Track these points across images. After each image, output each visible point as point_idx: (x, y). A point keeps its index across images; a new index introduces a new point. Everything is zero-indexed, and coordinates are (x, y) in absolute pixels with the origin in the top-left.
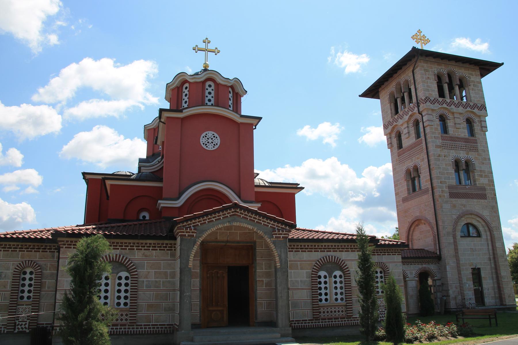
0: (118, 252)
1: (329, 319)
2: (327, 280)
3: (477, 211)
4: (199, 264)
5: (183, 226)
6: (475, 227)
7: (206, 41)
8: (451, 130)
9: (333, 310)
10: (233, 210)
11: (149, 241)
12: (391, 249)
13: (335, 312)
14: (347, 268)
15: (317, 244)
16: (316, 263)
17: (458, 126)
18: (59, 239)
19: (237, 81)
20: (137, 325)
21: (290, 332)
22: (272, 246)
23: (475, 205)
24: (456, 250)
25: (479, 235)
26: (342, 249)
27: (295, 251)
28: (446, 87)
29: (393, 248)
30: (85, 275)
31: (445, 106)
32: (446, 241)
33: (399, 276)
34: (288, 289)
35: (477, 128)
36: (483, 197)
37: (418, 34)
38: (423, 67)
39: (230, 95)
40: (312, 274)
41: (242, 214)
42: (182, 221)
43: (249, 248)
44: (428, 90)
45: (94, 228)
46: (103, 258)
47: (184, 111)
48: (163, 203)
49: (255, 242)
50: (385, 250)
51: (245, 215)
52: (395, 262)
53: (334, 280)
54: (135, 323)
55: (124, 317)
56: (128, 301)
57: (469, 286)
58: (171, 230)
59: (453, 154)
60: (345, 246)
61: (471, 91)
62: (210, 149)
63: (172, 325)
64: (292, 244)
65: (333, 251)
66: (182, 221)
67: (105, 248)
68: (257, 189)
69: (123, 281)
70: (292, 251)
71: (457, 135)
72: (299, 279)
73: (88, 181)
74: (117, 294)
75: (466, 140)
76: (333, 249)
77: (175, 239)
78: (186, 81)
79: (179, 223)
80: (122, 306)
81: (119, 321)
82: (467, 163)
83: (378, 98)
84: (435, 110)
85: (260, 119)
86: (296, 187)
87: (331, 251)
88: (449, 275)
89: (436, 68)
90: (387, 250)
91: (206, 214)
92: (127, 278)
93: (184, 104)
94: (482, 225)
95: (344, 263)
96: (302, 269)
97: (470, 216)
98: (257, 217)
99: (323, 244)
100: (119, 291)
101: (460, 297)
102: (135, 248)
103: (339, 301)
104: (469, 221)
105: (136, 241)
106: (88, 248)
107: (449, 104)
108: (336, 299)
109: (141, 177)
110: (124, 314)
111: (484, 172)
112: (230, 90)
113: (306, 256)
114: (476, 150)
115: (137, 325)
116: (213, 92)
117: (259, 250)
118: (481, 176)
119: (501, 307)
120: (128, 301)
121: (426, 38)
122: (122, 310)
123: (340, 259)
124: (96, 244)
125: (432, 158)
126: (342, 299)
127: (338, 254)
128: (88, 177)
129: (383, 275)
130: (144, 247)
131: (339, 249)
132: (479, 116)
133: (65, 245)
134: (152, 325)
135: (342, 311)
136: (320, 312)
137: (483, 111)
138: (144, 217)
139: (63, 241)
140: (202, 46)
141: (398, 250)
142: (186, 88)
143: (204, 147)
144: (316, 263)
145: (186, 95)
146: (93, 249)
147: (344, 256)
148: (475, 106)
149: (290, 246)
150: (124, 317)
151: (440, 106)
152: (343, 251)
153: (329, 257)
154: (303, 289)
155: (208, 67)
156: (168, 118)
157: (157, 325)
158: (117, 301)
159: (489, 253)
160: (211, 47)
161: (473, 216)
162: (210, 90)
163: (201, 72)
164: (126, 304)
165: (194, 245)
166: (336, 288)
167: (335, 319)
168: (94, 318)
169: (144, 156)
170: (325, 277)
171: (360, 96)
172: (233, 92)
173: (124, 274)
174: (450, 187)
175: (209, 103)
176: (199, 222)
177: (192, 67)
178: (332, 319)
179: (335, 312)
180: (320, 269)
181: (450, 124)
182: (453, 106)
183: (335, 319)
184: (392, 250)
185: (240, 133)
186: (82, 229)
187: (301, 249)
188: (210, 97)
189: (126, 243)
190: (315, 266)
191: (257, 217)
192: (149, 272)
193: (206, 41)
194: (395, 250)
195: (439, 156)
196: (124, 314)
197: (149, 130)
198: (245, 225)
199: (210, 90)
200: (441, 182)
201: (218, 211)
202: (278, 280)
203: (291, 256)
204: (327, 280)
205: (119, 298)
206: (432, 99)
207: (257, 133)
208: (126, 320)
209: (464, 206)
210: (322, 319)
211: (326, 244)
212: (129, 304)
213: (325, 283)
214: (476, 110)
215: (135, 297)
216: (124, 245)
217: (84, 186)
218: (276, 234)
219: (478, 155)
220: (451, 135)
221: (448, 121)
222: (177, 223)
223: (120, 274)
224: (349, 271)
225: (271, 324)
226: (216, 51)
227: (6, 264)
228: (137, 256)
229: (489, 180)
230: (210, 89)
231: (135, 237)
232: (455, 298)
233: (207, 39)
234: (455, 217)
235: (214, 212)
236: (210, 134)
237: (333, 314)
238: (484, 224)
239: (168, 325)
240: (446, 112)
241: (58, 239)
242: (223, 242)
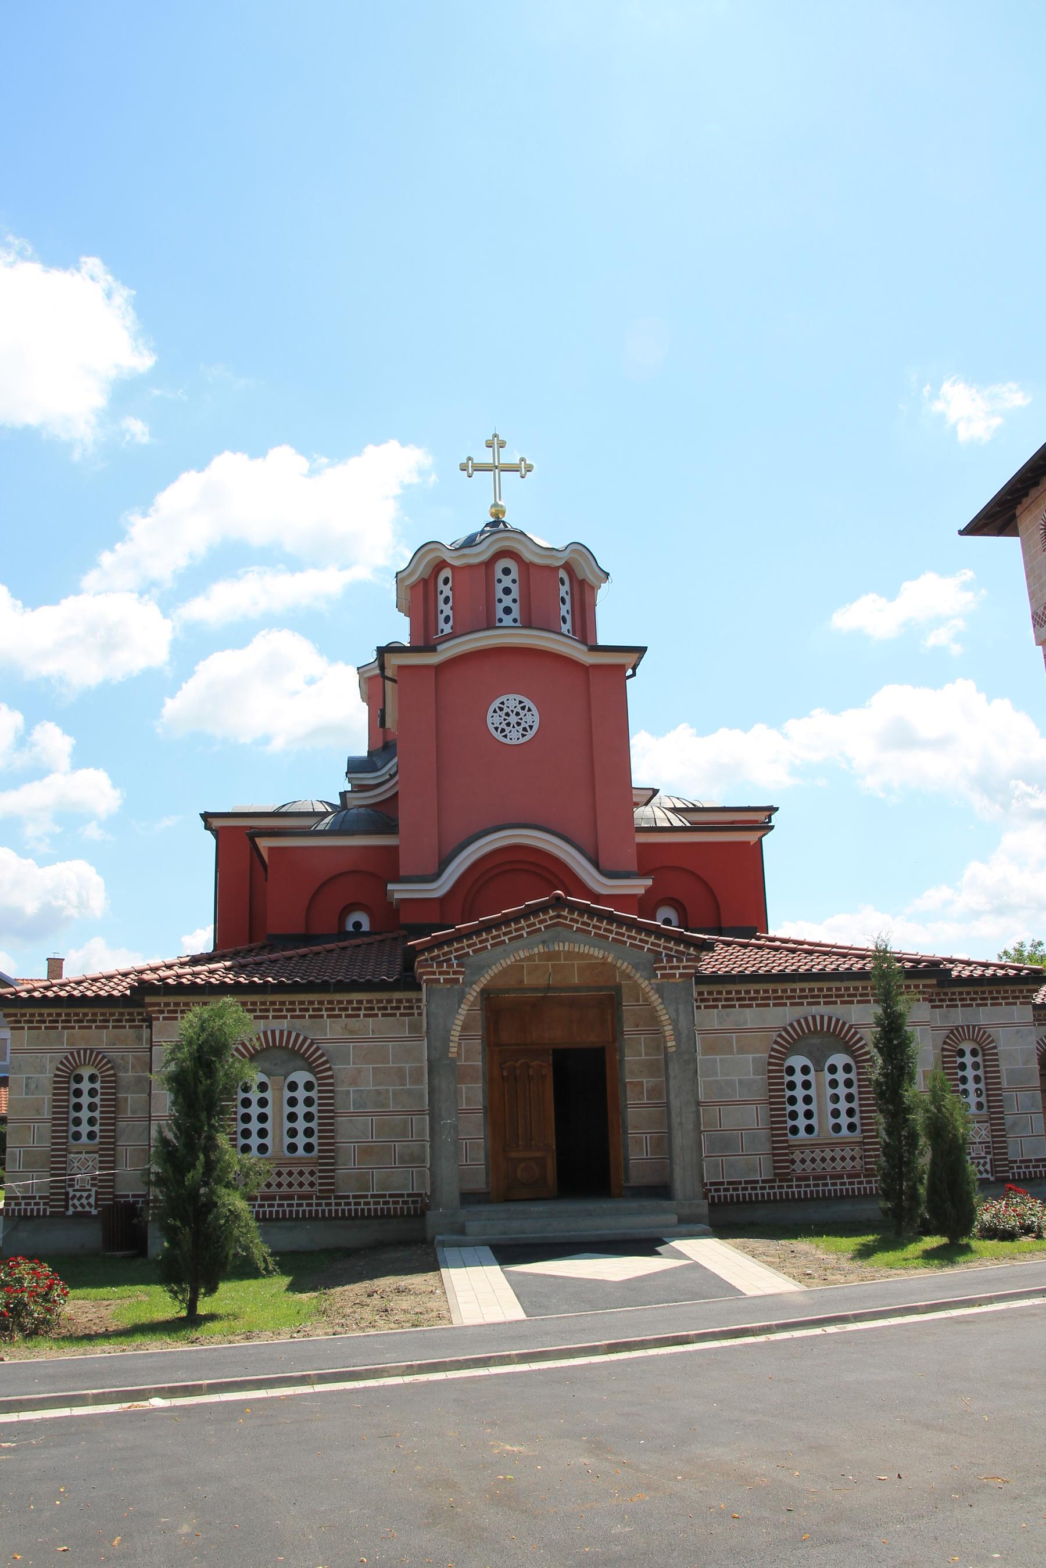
0: (285, 1024)
1: (815, 1178)
2: (811, 1077)
4: (480, 1048)
5: (432, 959)
7: (496, 443)
9: (828, 1154)
10: (552, 913)
11: (355, 996)
12: (1001, 988)
13: (843, 1159)
15: (779, 987)
16: (780, 1036)
18: (148, 1000)
19: (580, 549)
20: (336, 1197)
21: (705, 1210)
22: (654, 997)
26: (849, 996)
27: (723, 1006)
29: (1007, 987)
30: (200, 1087)
33: (1026, 1063)
34: (698, 1104)
39: (564, 590)
40: (770, 1064)
41: (577, 922)
42: (429, 948)
43: (607, 1001)
45: (226, 968)
46: (237, 1050)
47: (439, 648)
48: (399, 891)
49: (618, 988)
50: (983, 992)
51: (583, 923)
52: (1013, 1025)
53: (829, 1077)
54: (332, 1191)
55: (306, 1179)
56: (314, 1140)
58: (408, 967)
60: (856, 988)
62: (515, 742)
63: (420, 1195)
64: (705, 988)
65: (825, 1003)
66: (429, 948)
67: (240, 1023)
68: (641, 838)
69: (301, 1094)
70: (717, 1007)
73: (217, 833)
74: (288, 1125)
76: (825, 996)
77: (420, 989)
78: (442, 564)
79: (421, 952)
80: (301, 1151)
81: (296, 1188)
85: (642, 650)
86: (759, 820)
87: (819, 1003)
90: (991, 992)
91: (487, 927)
92: (309, 1086)
93: (442, 625)
95: (856, 1033)
96: (742, 1050)
98: (614, 927)
99: (798, 986)
100: (292, 1117)
102: (325, 1013)
103: (845, 1130)
105: (326, 997)
106: (203, 1029)
108: (837, 1128)
109: (345, 817)
110: (306, 1170)
112: (562, 574)
113: (751, 1017)
115: (336, 1197)
116: (515, 588)
117: (628, 1006)
120: (314, 1140)
122: (300, 1162)
123: (844, 1024)
124: (219, 1022)
126: (851, 1127)
127: (838, 1010)
128: (217, 823)
129: (979, 1059)
130: (346, 1009)
131: (842, 996)
133: (162, 1012)
134: (373, 1196)
135: (853, 1158)
136: (793, 1162)
138: (357, 925)
139: (159, 1005)
140: (485, 457)
141: (1021, 991)
142: (446, 581)
143: (498, 736)
144: (780, 1036)
145: (446, 600)
146: (212, 1035)
149: (700, 993)
150: (306, 1179)
152: (852, 1002)
153: (814, 1018)
154: (745, 1103)
155: (504, 513)
156: (400, 667)
157: (384, 1196)
158: (288, 1140)
160: (508, 457)
162: (507, 581)
163: (482, 532)
164: (309, 1148)
165: (460, 1003)
166: (835, 1099)
167: (832, 1177)
168: (219, 1181)
169: (362, 751)
170: (805, 1070)
171: (961, 533)
172: (566, 584)
173: (301, 1077)
175: (508, 620)
176: (469, 946)
177: (456, 523)
178: (824, 1178)
179: (833, 1159)
180: (793, 1048)
183: (832, 1177)
184: (1006, 992)
185: (595, 689)
186: (199, 973)
187: (739, 999)
188: (507, 601)
189: (302, 1003)
190: (776, 1042)
191: (614, 927)
192: (359, 1071)
193: (496, 443)
194: (1013, 991)
196: (306, 1170)
197: (370, 678)
198: (585, 949)
199: (507, 581)
201: (516, 918)
202: (672, 1082)
203: (710, 1019)
204: (811, 1077)
205: (293, 1133)
207: (638, 690)
208: (312, 1184)
210: (799, 1179)
211: (806, 985)
212: (316, 1148)
213: (806, 1085)
215: (328, 1131)
216: (297, 1007)
217: (209, 841)
218: (664, 968)
222: (415, 952)
223: (292, 1078)
225: (662, 1191)
226: (521, 468)
228: (329, 1031)
230: (507, 581)
231: (324, 987)
233: (495, 436)
235: (506, 920)
236: (512, 701)
237: (839, 1165)
239: (409, 1195)
241: (144, 998)
242: (536, 989)
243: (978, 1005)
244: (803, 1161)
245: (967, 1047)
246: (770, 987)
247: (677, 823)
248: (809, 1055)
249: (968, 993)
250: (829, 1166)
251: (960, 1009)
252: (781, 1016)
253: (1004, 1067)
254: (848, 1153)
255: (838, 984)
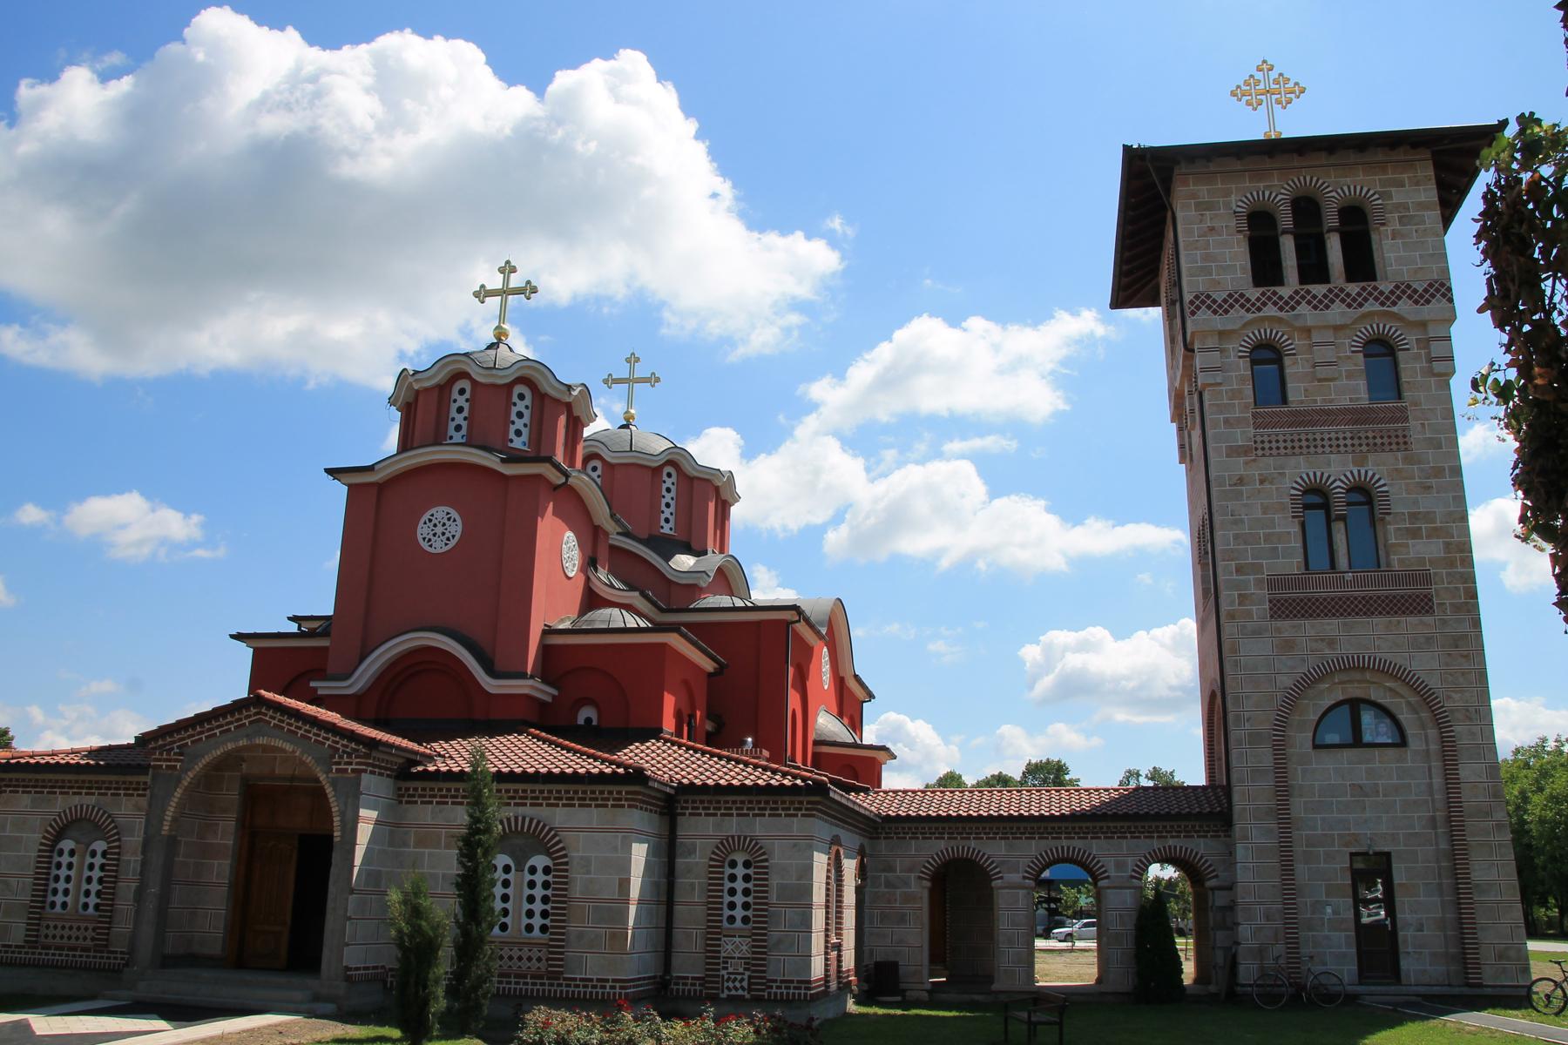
0: (91, 800)
2: (510, 876)
3: (1389, 657)
6: (1384, 711)
8: (1297, 392)
9: (516, 953)
10: (253, 710)
14: (563, 849)
17: (1322, 372)
23: (1375, 637)
24: (1283, 791)
25: (1402, 742)
28: (1288, 246)
31: (1270, 311)
32: (1250, 760)
35: (1411, 367)
36: (1422, 605)
37: (1259, 76)
38: (1194, 196)
44: (1206, 271)
52: (791, 837)
53: (528, 877)
55: (90, 934)
57: (1334, 912)
59: (1298, 470)
61: (1387, 243)
71: (1319, 402)
72: (440, 872)
75: (1357, 416)
82: (1363, 493)
83: (1154, 301)
84: (1233, 331)
88: (1243, 876)
89: (1238, 195)
90: (767, 802)
94: (1409, 703)
97: (1357, 676)
101: (1280, 949)
103: (536, 932)
104: (1355, 691)
107: (1290, 304)
108: (529, 928)
111: (1428, 517)
114: (1401, 442)
118: (1415, 534)
119: (1466, 991)
121: (1291, 85)
125: (1214, 490)
127: (543, 812)
132: (1423, 325)
135: (539, 960)
137: (1437, 305)
140: (496, 282)
147: (559, 816)
148: (1404, 290)
150: (90, 934)
151: (1250, 316)
155: (507, 336)
159: (1433, 801)
161: (1368, 676)
174: (1274, 583)
175: (458, 437)
179: (520, 958)
181: (1292, 368)
182: (1303, 309)
194: (792, 803)
195: (1241, 481)
198: (279, 743)
200: (1239, 570)
204: (510, 876)
206: (1220, 296)
209: (1331, 643)
214: (1404, 307)
219: (1407, 460)
220: (1293, 407)
221: (1287, 361)
223: (93, 847)
224: (565, 856)
227: (27, 819)
229: (1447, 545)
232: (1261, 952)
234: (1287, 681)
238: (1413, 699)
240: (1280, 334)
243: (755, 815)
244: (530, 959)
245: (740, 858)
246: (562, 787)
247: (642, 625)
248: (512, 855)
249: (702, 802)
250: (515, 964)
251: (735, 819)
252: (62, 804)
253: (775, 881)
254: (535, 953)
255: (542, 787)
